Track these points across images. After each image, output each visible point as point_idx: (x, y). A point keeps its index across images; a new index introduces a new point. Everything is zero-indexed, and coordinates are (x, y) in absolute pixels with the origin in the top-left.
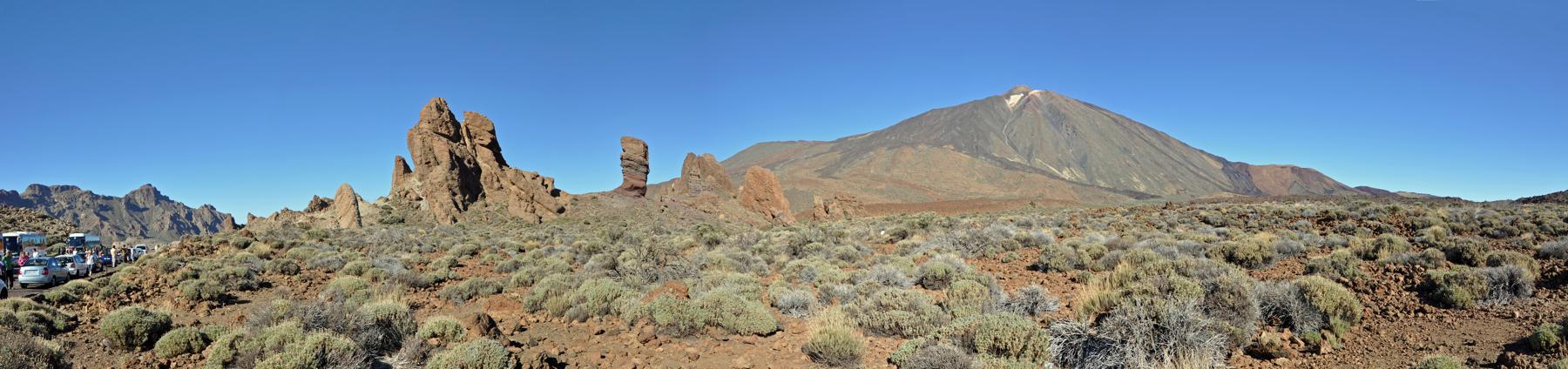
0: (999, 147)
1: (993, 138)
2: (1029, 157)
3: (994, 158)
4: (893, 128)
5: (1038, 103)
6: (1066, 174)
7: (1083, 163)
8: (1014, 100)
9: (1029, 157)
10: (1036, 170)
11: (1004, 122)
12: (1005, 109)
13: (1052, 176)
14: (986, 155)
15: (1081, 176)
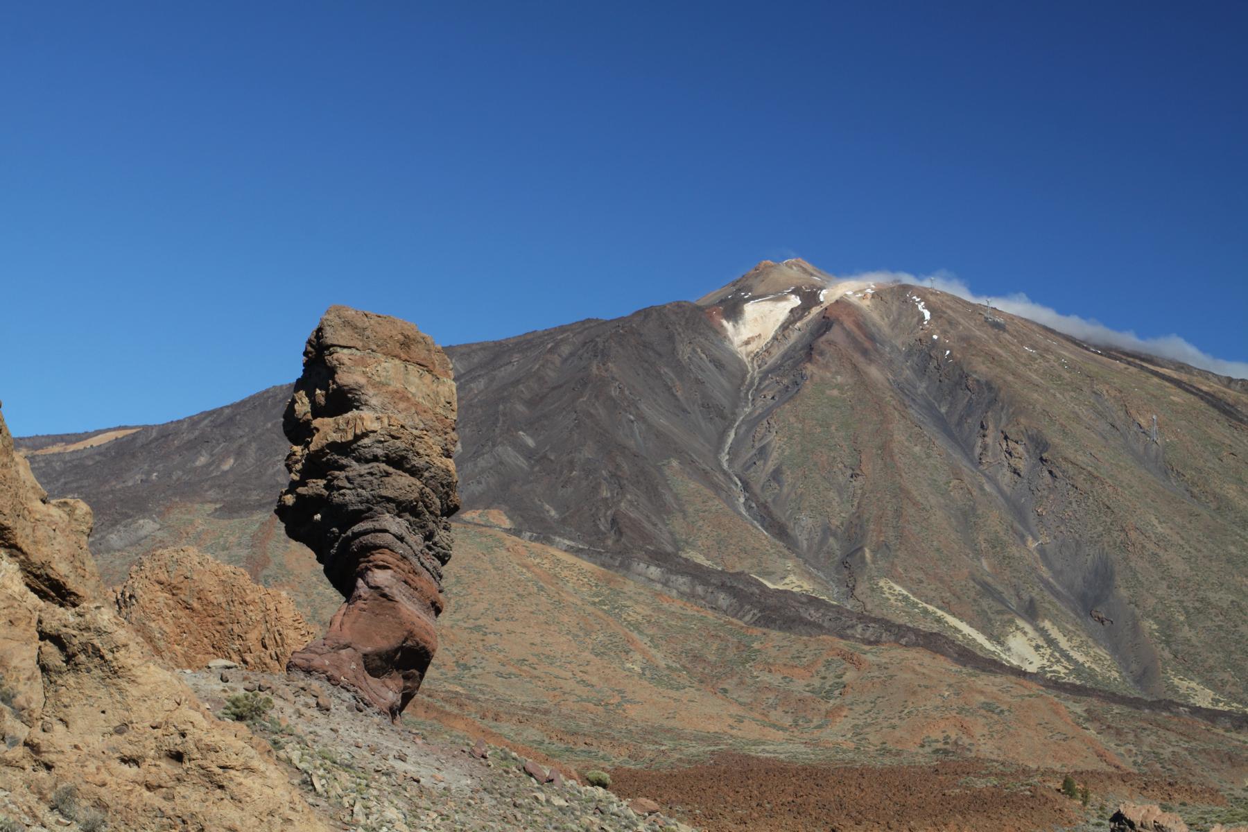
0: (713, 527)
1: (681, 482)
2: (848, 566)
3: (697, 573)
4: (222, 423)
5: (866, 341)
6: (1022, 649)
7: (1094, 602)
8: (759, 324)
9: (848, 566)
10: (899, 633)
11: (721, 416)
12: (725, 363)
13: (966, 656)
14: (658, 557)
15: (1092, 658)
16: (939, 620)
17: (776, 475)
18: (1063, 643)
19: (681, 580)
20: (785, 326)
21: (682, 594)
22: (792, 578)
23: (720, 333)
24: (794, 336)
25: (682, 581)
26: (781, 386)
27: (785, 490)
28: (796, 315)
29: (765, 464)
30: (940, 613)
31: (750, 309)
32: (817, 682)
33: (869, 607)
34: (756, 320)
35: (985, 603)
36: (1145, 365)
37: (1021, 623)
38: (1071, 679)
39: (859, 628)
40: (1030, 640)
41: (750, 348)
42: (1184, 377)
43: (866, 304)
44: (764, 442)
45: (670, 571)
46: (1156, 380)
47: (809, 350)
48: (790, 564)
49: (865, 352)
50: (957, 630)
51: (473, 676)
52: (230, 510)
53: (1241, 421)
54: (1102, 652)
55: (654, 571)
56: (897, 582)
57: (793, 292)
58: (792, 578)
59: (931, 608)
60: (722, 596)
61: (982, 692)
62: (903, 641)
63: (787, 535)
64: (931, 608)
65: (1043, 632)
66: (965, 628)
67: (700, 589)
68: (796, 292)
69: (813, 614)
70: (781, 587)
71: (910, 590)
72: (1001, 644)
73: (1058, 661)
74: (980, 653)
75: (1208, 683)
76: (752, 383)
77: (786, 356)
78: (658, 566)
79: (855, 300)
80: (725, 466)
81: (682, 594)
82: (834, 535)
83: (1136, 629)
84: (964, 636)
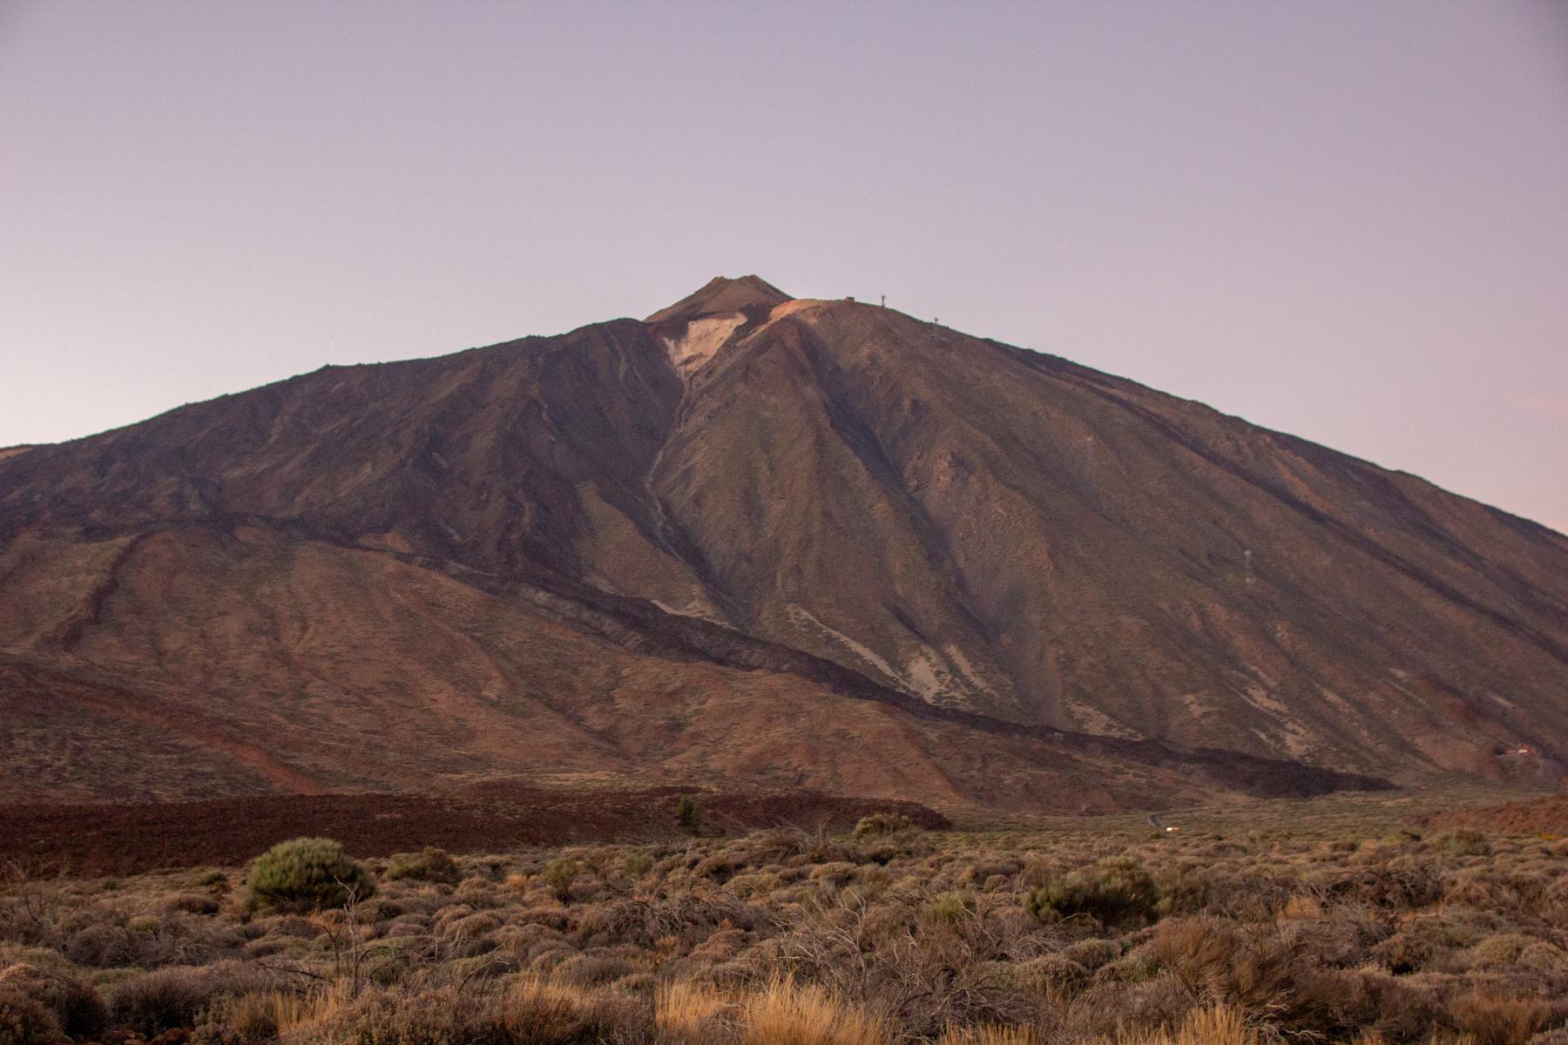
3: (592, 600)
6: (923, 676)
12: (664, 382)
13: (855, 683)
16: (842, 646)
17: (698, 500)
18: (965, 667)
19: (569, 605)
20: (729, 346)
21: (565, 618)
22: (696, 603)
23: (663, 354)
24: (738, 355)
25: (567, 606)
26: (715, 405)
27: (705, 513)
28: (741, 332)
29: (687, 486)
30: (844, 638)
31: (695, 328)
32: (677, 709)
33: (771, 632)
34: (700, 339)
35: (897, 629)
36: (1096, 386)
37: (925, 648)
38: (966, 707)
39: (745, 654)
40: (932, 666)
41: (692, 367)
42: (1134, 399)
43: (813, 321)
44: (690, 463)
45: (560, 595)
46: (1103, 401)
47: (747, 371)
48: (696, 589)
49: (803, 372)
50: (859, 656)
51: (311, 706)
52: (91, 533)
53: (1184, 444)
54: (1007, 680)
55: (542, 597)
56: (807, 609)
57: (742, 310)
58: (696, 603)
59: (835, 633)
60: (608, 621)
61: (838, 718)
62: (785, 667)
63: (702, 560)
64: (835, 633)
65: (947, 660)
66: (868, 655)
67: (586, 615)
68: (746, 310)
69: (699, 640)
70: (678, 613)
71: (818, 616)
72: (903, 670)
73: (957, 686)
74: (874, 679)
75: (1103, 709)
76: (687, 404)
77: (724, 376)
78: (548, 591)
79: (802, 317)
80: (648, 486)
81: (565, 618)
82: (749, 559)
83: (1041, 658)
84: (864, 662)
